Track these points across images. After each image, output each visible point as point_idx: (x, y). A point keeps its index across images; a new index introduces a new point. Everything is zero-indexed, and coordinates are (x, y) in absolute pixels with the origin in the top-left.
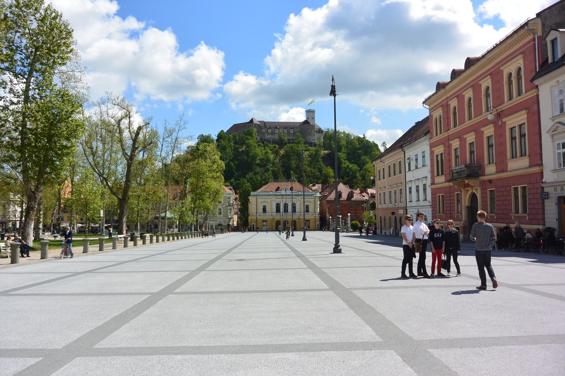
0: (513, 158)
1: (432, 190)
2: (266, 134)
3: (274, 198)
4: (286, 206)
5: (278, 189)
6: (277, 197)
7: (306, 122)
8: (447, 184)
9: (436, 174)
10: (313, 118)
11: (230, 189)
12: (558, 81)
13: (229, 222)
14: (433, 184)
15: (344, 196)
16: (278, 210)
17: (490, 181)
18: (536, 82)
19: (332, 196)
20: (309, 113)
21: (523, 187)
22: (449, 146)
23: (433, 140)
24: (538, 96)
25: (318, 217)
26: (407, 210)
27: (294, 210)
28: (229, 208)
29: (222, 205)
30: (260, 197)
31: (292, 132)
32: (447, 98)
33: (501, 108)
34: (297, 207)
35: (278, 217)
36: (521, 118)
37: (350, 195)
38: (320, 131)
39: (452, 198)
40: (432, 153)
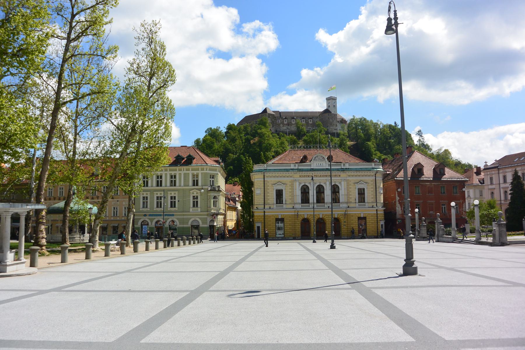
2: (281, 125)
3: (297, 175)
4: (320, 190)
5: (304, 159)
6: (304, 173)
7: (327, 111)
10: (335, 106)
11: (217, 161)
13: (213, 221)
16: (305, 199)
20: (329, 101)
25: (381, 212)
27: (335, 199)
28: (213, 194)
29: (200, 189)
30: (271, 174)
31: (311, 123)
35: (306, 212)
38: (343, 121)
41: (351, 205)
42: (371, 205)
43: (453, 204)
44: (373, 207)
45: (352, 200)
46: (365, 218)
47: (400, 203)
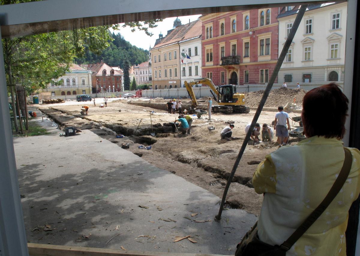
0: (261, 55)
1: (203, 69)
8: (215, 67)
9: (206, 60)
12: (290, 21)
14: (203, 65)
15: (108, 73)
17: (246, 66)
18: (279, 19)
19: (100, 73)
21: (266, 70)
22: (218, 46)
23: (204, 41)
24: (278, 26)
26: (181, 81)
32: (217, 18)
33: (255, 29)
34: (76, 81)
36: (268, 35)
37: (112, 72)
39: (218, 74)
40: (203, 48)
41: (80, 86)
42: (87, 86)
43: (110, 86)
44: (88, 86)
45: (80, 84)
46: (85, 91)
47: (98, 84)
